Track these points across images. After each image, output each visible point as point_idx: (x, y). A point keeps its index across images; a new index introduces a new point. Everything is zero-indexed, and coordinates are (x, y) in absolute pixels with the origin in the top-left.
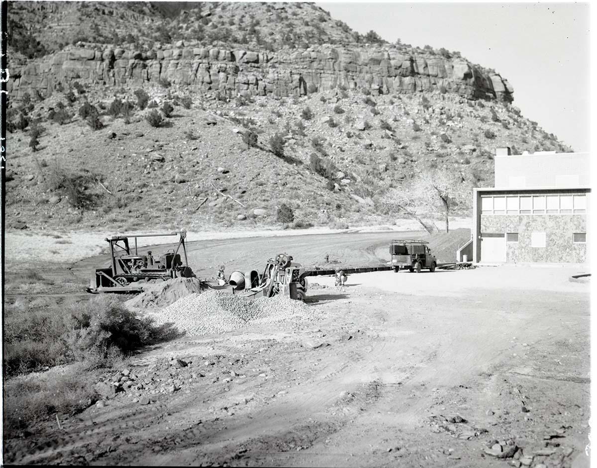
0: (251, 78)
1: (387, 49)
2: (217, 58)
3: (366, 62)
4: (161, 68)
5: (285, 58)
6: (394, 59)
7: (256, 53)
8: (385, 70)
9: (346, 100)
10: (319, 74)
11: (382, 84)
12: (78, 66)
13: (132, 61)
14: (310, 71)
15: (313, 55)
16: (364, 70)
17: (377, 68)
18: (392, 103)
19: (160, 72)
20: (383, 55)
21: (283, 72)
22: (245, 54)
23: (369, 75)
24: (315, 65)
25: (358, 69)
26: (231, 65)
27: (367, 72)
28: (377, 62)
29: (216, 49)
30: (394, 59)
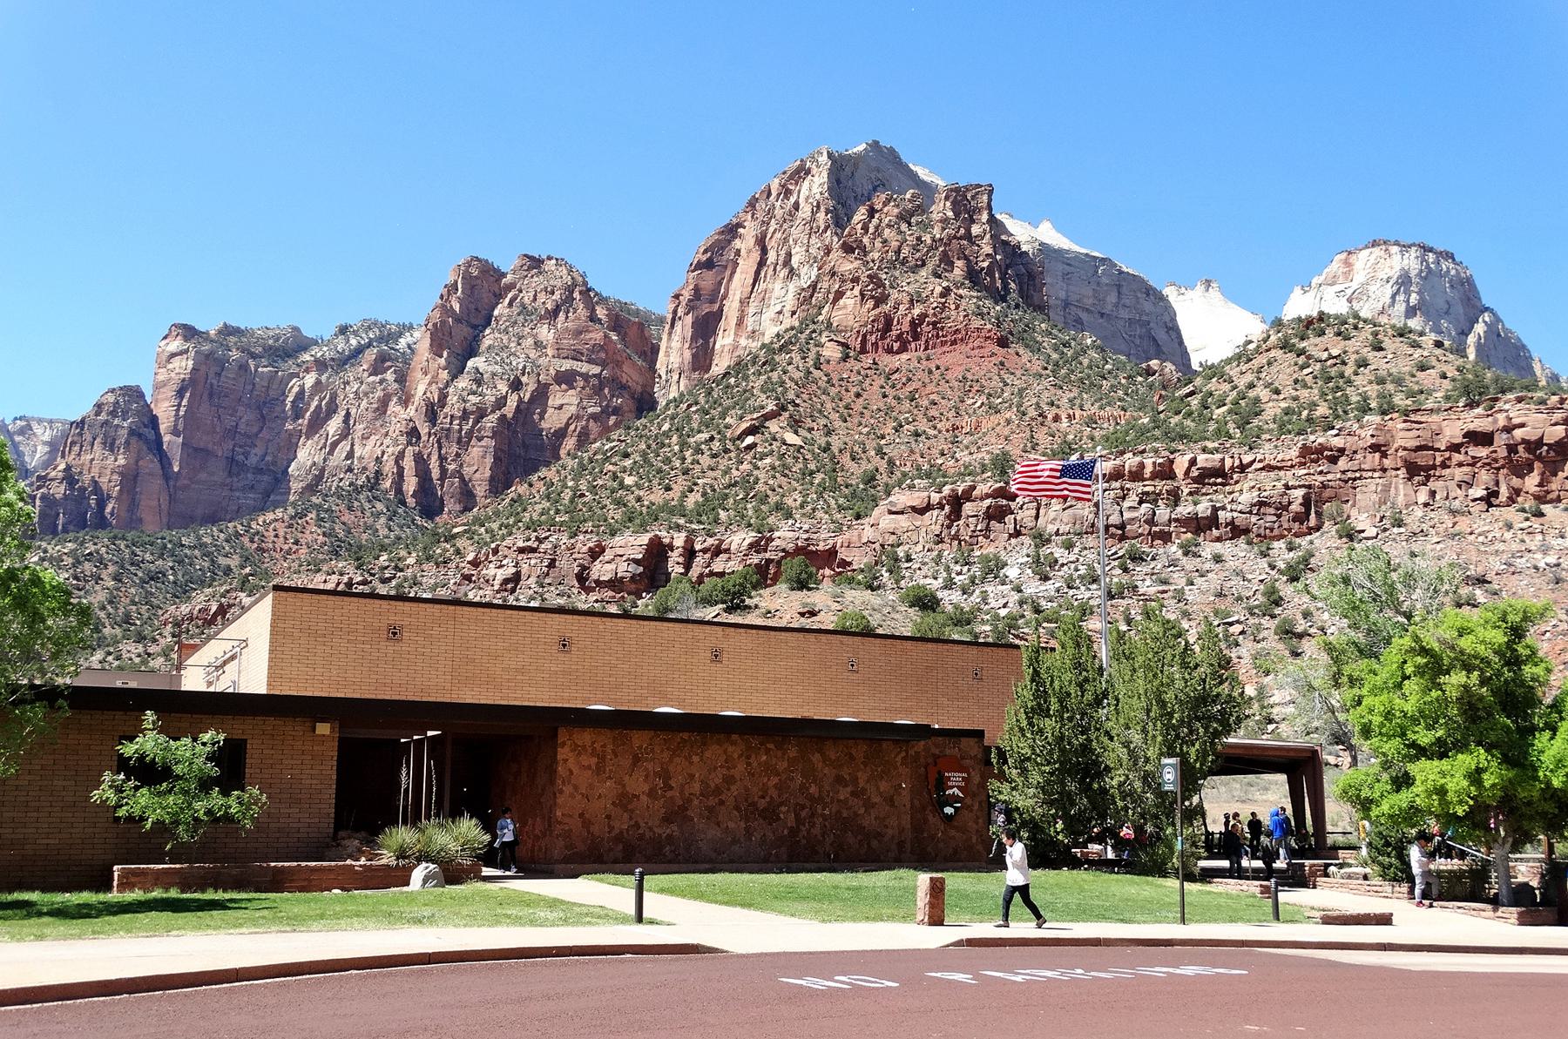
0: (1204, 508)
1: (1507, 407)
2: (1137, 475)
3: (1459, 440)
4: (1038, 509)
5: (1280, 457)
6: (1522, 425)
7: (1218, 456)
8: (1503, 453)
9: (1402, 530)
10: (1350, 481)
11: (1497, 483)
12: (903, 522)
13: (988, 502)
14: (1329, 477)
15: (1338, 442)
16: (1454, 462)
17: (1482, 452)
18: (1509, 526)
19: (1037, 517)
20: (1496, 421)
21: (1271, 485)
22: (1193, 462)
23: (1466, 469)
24: (1343, 463)
25: (1439, 460)
26: (1162, 486)
27: (1460, 465)
28: (1484, 439)
29: (1138, 459)
30: (1522, 425)
